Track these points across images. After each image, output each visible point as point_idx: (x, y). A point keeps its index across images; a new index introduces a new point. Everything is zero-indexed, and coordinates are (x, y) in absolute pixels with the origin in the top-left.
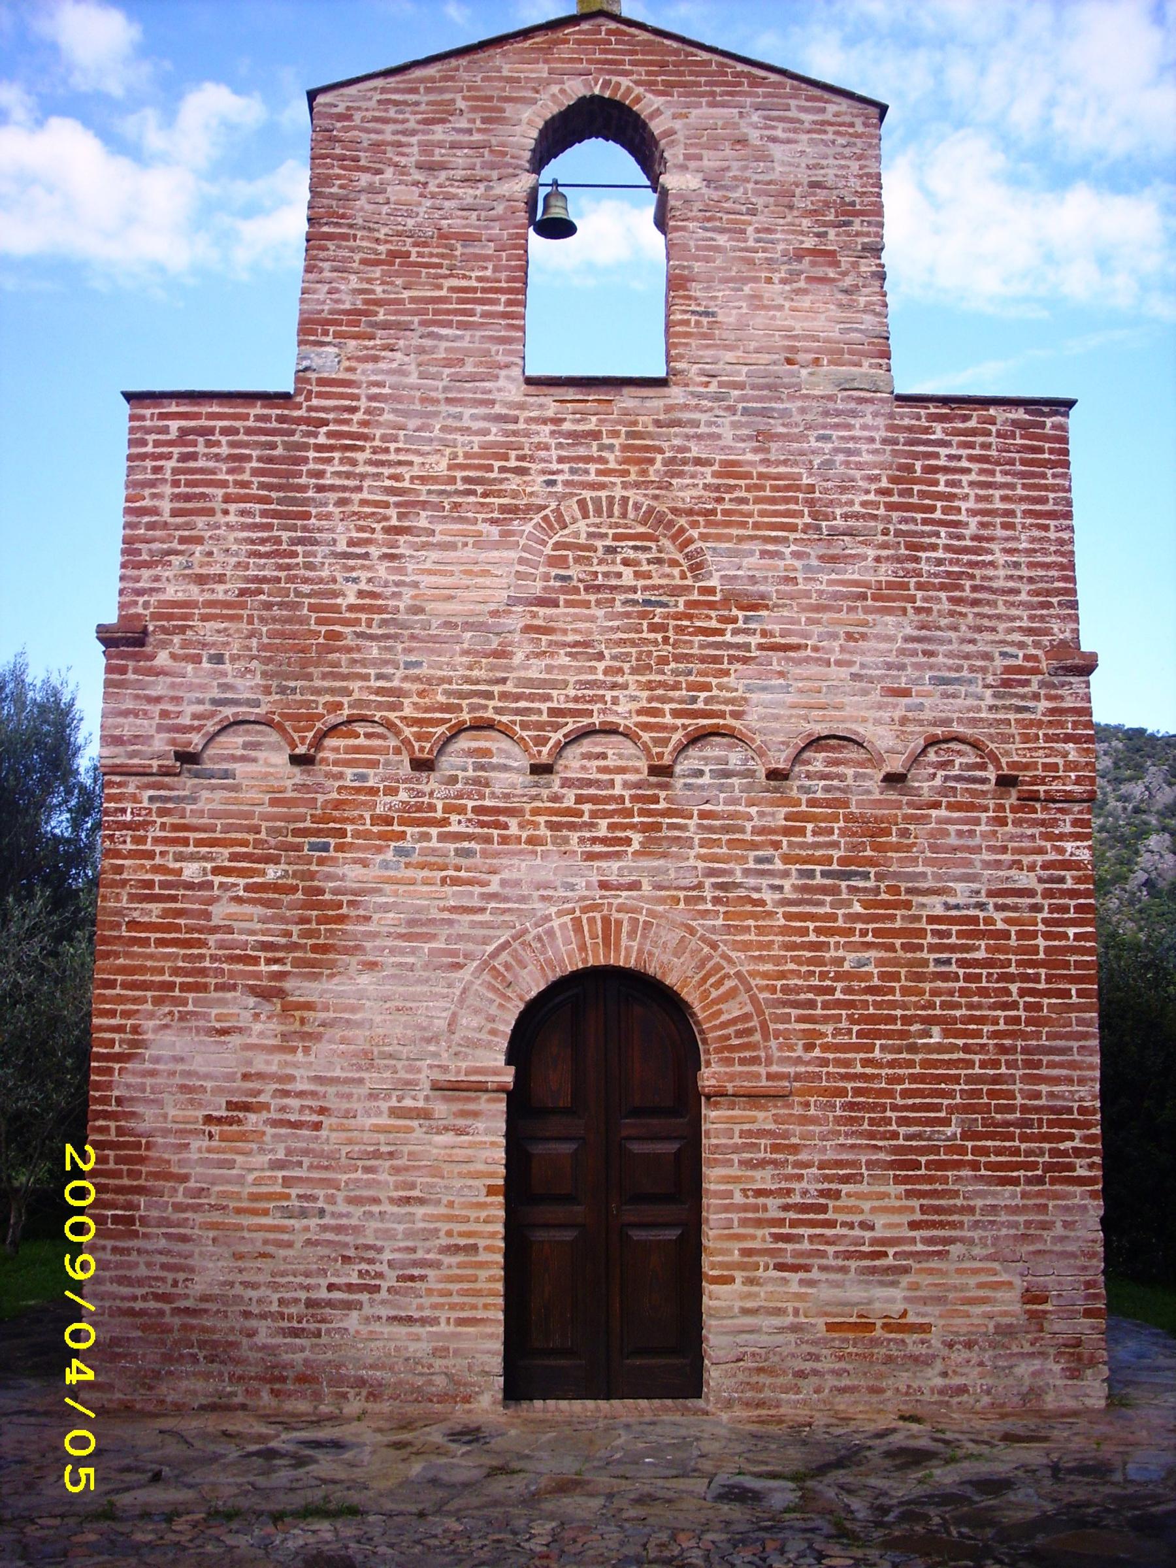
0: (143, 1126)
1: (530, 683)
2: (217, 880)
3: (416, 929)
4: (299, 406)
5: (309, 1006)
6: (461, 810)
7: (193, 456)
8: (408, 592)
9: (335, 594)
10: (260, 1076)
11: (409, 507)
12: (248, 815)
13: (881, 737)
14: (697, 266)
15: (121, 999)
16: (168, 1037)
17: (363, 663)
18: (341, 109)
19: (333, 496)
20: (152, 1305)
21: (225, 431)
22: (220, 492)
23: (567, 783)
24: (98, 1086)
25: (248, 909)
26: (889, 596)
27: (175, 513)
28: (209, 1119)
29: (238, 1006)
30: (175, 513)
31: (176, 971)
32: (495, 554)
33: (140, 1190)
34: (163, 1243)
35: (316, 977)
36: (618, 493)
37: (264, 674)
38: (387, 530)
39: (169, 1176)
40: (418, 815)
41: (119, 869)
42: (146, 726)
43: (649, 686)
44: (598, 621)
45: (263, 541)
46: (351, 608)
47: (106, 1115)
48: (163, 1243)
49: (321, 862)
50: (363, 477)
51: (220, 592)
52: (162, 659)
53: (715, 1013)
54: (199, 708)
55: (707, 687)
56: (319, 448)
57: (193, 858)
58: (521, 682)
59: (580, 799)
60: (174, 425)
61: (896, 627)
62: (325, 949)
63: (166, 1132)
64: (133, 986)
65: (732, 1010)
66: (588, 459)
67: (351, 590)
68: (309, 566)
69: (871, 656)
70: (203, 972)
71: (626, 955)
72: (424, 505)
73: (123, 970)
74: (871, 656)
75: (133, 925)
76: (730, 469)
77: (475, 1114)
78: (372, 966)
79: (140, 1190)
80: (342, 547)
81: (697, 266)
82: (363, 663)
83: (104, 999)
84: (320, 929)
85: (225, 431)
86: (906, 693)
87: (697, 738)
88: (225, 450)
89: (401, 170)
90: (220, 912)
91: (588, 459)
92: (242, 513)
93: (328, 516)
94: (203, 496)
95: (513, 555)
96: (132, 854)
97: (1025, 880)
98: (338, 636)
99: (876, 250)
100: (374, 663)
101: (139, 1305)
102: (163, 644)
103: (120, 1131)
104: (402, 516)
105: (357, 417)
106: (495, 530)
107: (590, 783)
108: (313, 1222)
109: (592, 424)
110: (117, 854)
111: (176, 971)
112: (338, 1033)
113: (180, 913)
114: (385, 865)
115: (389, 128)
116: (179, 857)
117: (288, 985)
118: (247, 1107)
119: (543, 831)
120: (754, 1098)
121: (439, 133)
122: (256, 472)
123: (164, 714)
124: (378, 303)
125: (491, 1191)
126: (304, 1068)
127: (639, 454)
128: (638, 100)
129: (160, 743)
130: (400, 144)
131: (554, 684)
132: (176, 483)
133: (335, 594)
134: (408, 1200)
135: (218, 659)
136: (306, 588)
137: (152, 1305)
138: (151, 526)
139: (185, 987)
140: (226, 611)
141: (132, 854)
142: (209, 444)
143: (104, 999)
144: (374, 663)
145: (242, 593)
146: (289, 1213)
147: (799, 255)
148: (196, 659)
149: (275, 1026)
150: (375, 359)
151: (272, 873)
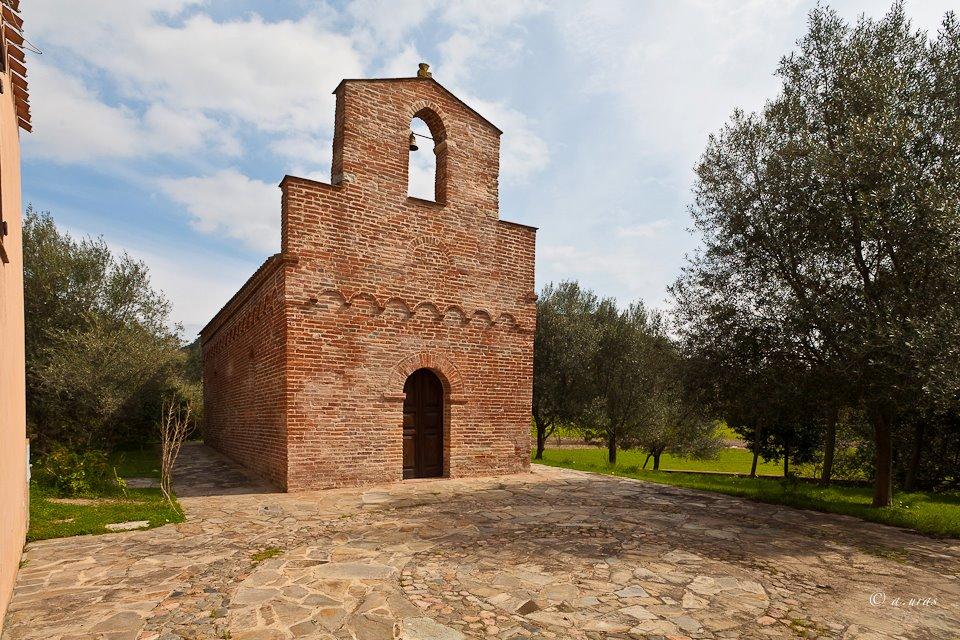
0: (304, 411)
1: (410, 289)
2: (323, 339)
3: (380, 355)
4: (343, 192)
5: (351, 376)
6: (391, 323)
7: (311, 203)
8: (377, 258)
9: (356, 255)
10: (338, 396)
11: (378, 231)
12: (332, 320)
13: (492, 312)
14: (454, 171)
15: (296, 373)
16: (310, 384)
17: (364, 277)
18: (354, 89)
19: (355, 224)
20: (309, 462)
21: (321, 196)
22: (320, 217)
23: (418, 318)
24: (290, 399)
25: (334, 348)
26: (494, 275)
27: (305, 221)
28: (324, 408)
29: (331, 376)
30: (305, 221)
31: (312, 365)
32: (401, 250)
33: (304, 429)
34: (311, 444)
35: (353, 368)
36: (433, 237)
37: (336, 277)
38: (371, 238)
39: (312, 425)
40: (380, 324)
41: (293, 334)
42: (301, 290)
43: (439, 293)
44: (426, 273)
45: (334, 235)
46: (361, 260)
47: (292, 408)
48: (311, 444)
49: (353, 335)
50: (364, 219)
51: (321, 249)
52: (303, 269)
53: (454, 381)
54: (316, 285)
55: (452, 295)
56: (351, 208)
57: (316, 331)
58: (408, 288)
59: (422, 322)
60: (304, 190)
61: (496, 283)
62: (355, 360)
63: (311, 412)
64: (300, 369)
65: (456, 380)
66: (425, 225)
67: (361, 254)
68: (349, 246)
69: (491, 290)
70: (320, 365)
71: (431, 366)
72: (381, 232)
73: (296, 364)
74: (491, 290)
75: (298, 351)
76: (460, 235)
77: (395, 406)
78: (368, 366)
79: (304, 429)
80: (357, 241)
81: (454, 171)
82: (364, 277)
83: (290, 373)
84: (355, 354)
85: (321, 196)
86: (496, 301)
87: (451, 308)
88: (321, 203)
89: (373, 118)
90: (325, 347)
91: (425, 225)
92: (328, 225)
93: (353, 230)
94: (315, 217)
95: (405, 251)
96: (296, 329)
97: (520, 350)
98: (358, 268)
99: (496, 177)
100: (367, 278)
101: (305, 462)
102: (305, 264)
103: (297, 412)
104: (375, 235)
105: (361, 199)
106: (401, 243)
107: (423, 318)
108: (353, 436)
109: (426, 215)
110: (292, 329)
111: (312, 365)
112: (359, 384)
113: (312, 348)
114: (371, 337)
115: (369, 101)
116: (311, 331)
117: (345, 370)
118: (335, 405)
119: (412, 331)
120: (461, 403)
121: (384, 108)
122: (331, 212)
123: (306, 286)
124: (367, 162)
125: (399, 426)
126: (349, 394)
127: (437, 227)
128: (440, 112)
129: (305, 295)
130: (372, 108)
131: (415, 290)
132: (306, 211)
133: (356, 255)
134: (377, 430)
135: (321, 271)
136: (348, 252)
137: (309, 462)
138: (299, 224)
139: (315, 370)
140: (324, 255)
141: (296, 329)
142: (316, 199)
143: (290, 373)
144: (367, 278)
145: (329, 250)
146: (346, 434)
147: (477, 174)
148: (314, 270)
149: (341, 382)
150: (367, 182)
151: (340, 337)
